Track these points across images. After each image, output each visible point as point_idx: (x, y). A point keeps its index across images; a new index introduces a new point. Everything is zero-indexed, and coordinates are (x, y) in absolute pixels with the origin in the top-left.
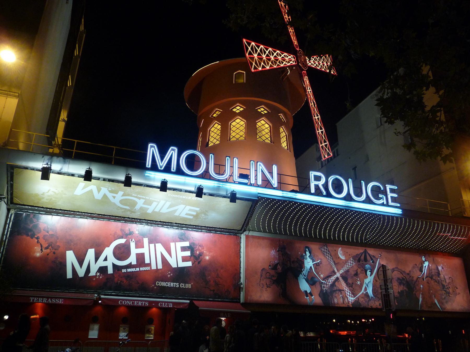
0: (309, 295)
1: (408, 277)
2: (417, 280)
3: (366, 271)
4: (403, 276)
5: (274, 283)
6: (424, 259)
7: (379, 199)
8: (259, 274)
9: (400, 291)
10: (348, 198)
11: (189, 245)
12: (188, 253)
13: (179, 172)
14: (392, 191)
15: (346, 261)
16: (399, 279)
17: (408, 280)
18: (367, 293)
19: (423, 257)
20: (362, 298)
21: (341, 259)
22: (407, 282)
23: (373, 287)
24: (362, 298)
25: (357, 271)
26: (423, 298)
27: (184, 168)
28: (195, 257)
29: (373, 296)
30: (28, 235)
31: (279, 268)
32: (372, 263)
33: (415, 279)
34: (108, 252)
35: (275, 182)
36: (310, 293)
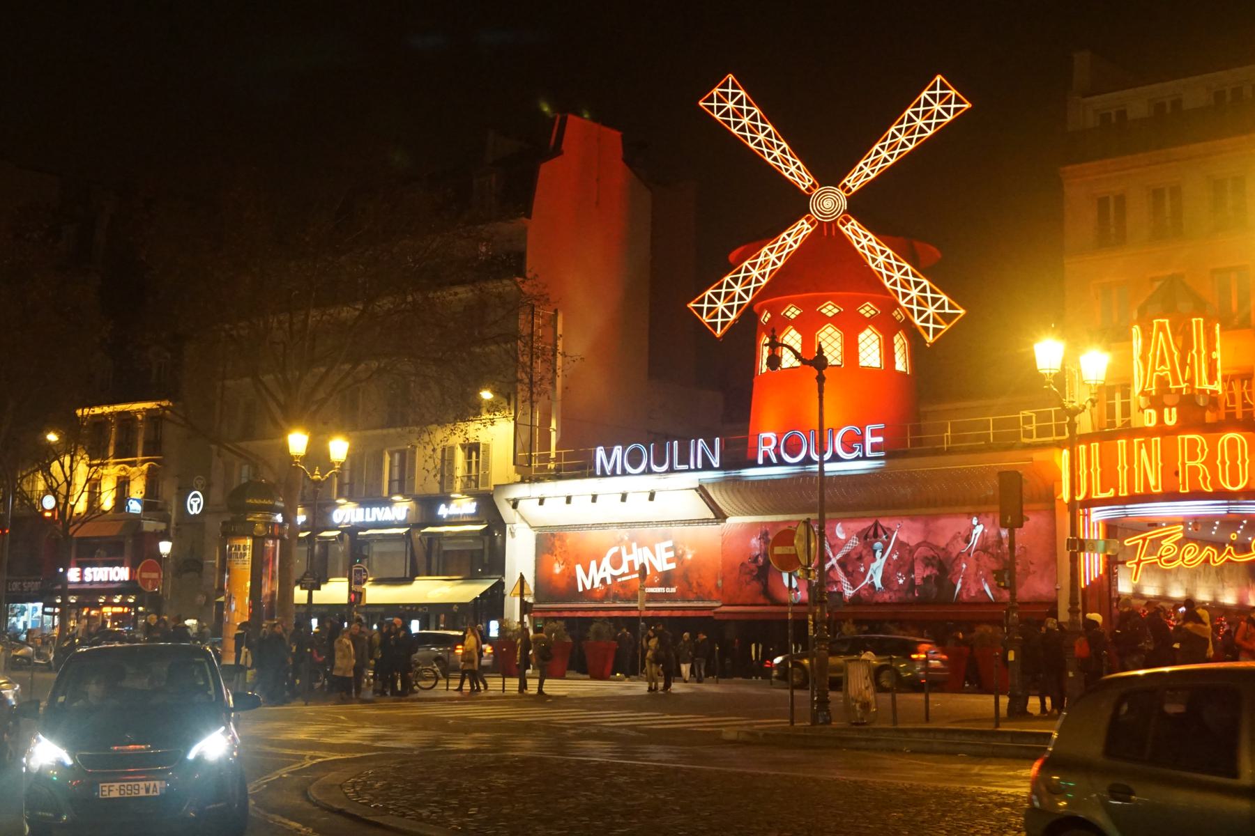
0: (795, 591)
1: (942, 555)
2: (958, 556)
3: (875, 552)
4: (932, 553)
5: (753, 580)
6: (975, 521)
7: (852, 450)
8: (738, 571)
9: (925, 576)
10: (808, 460)
11: (671, 545)
12: (671, 554)
13: (624, 473)
14: (874, 434)
15: (847, 541)
16: (926, 558)
17: (941, 558)
18: (873, 583)
19: (975, 518)
20: (865, 589)
21: (840, 539)
22: (940, 562)
23: (883, 573)
24: (865, 589)
25: (861, 553)
26: (963, 584)
27: (629, 469)
28: (678, 557)
29: (881, 586)
30: (549, 554)
31: (761, 560)
32: (886, 540)
33: (954, 555)
34: (606, 562)
35: (716, 462)
36: (796, 588)
